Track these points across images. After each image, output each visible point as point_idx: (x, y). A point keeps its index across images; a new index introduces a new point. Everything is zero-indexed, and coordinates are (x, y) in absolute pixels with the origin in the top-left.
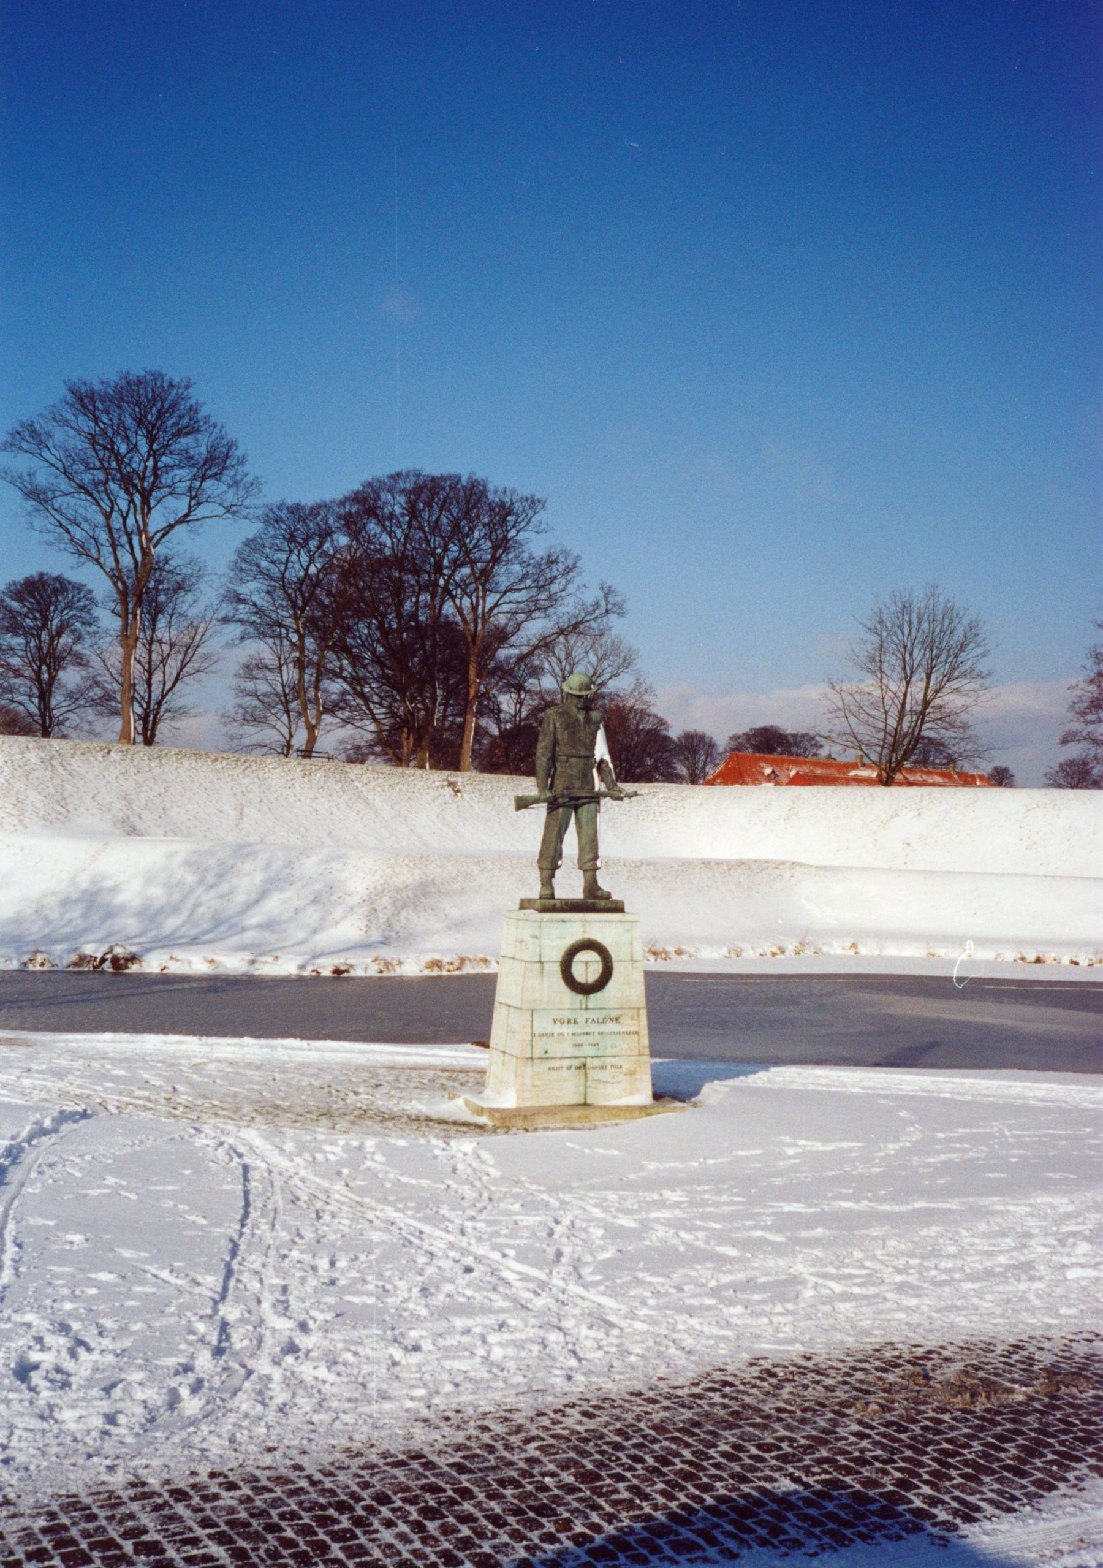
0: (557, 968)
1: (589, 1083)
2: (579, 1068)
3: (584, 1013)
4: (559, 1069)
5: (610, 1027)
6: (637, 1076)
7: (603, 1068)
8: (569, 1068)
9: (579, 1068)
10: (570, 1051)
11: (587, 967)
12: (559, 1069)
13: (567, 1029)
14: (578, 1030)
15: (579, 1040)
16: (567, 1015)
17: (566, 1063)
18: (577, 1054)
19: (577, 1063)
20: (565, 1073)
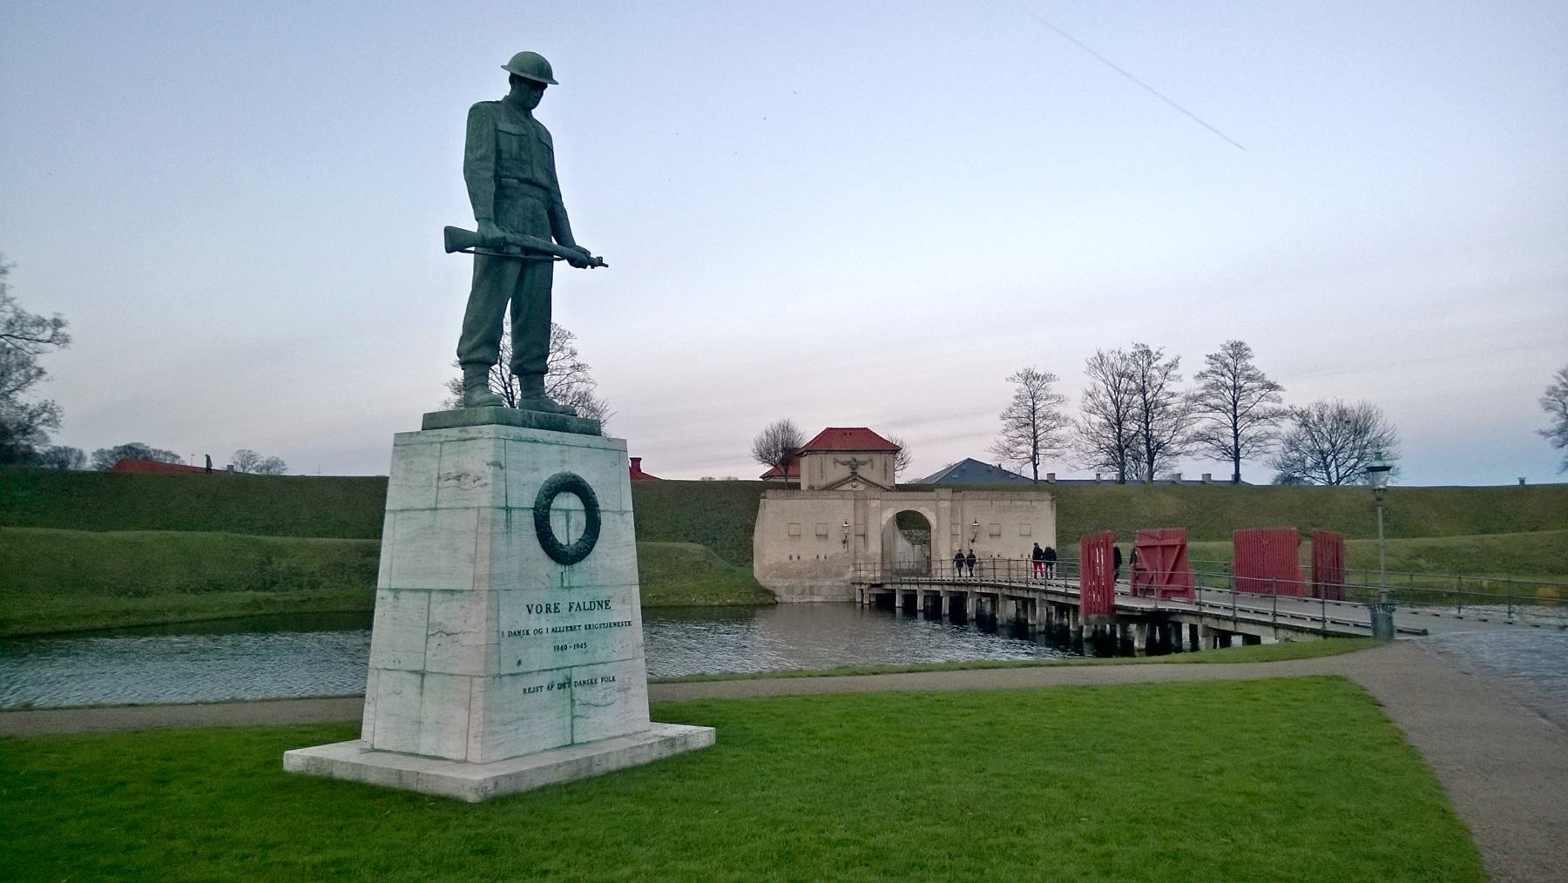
0: (529, 519)
1: (578, 710)
2: (561, 686)
3: (566, 592)
4: (537, 689)
5: (598, 617)
6: (632, 691)
7: (592, 682)
8: (550, 688)
9: (561, 686)
10: (551, 659)
11: (567, 525)
12: (537, 689)
13: (545, 622)
14: (561, 624)
15: (563, 639)
16: (544, 597)
17: (544, 680)
18: (562, 664)
19: (559, 678)
20: (545, 695)
